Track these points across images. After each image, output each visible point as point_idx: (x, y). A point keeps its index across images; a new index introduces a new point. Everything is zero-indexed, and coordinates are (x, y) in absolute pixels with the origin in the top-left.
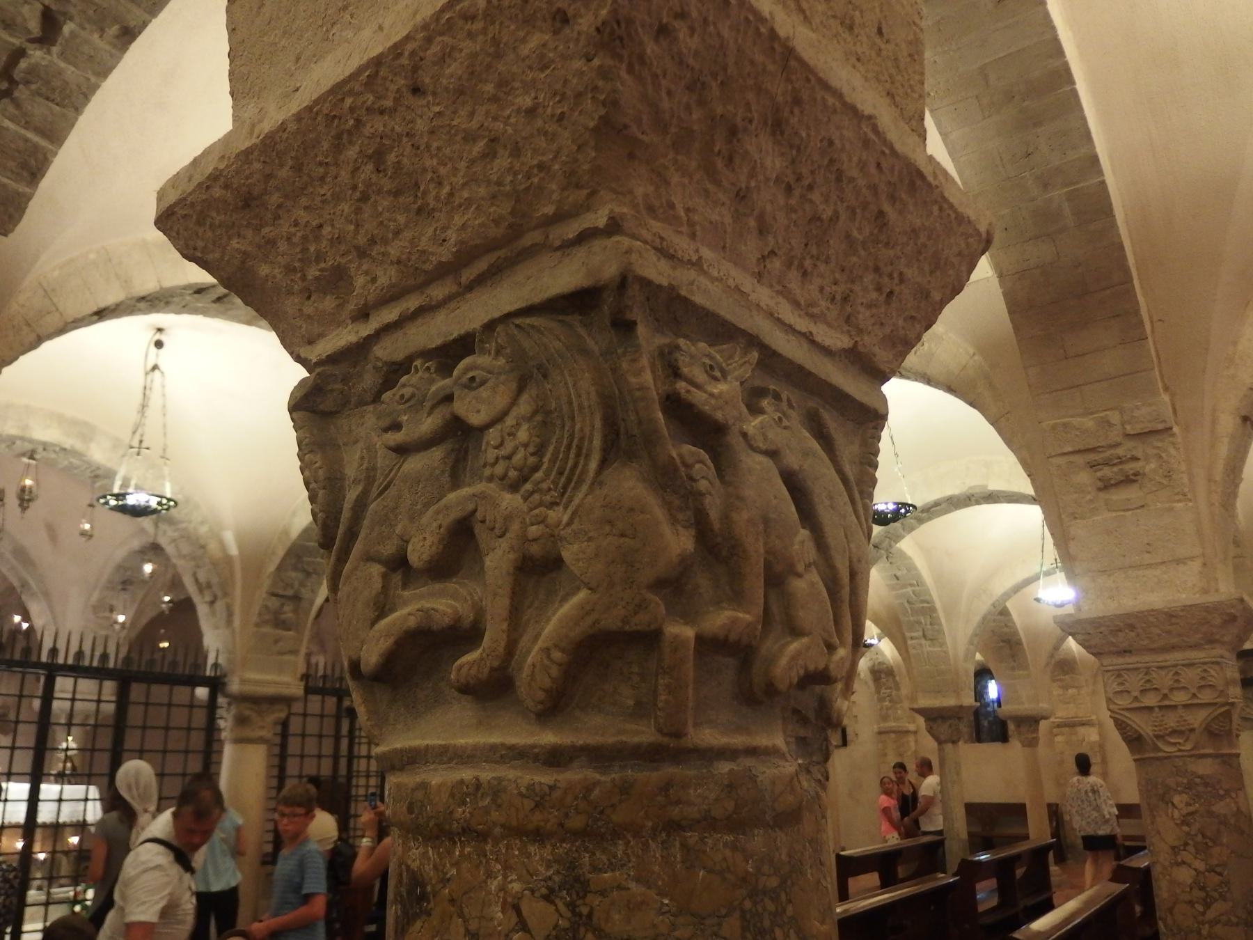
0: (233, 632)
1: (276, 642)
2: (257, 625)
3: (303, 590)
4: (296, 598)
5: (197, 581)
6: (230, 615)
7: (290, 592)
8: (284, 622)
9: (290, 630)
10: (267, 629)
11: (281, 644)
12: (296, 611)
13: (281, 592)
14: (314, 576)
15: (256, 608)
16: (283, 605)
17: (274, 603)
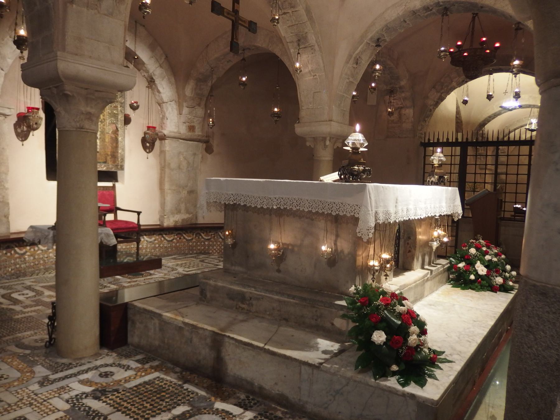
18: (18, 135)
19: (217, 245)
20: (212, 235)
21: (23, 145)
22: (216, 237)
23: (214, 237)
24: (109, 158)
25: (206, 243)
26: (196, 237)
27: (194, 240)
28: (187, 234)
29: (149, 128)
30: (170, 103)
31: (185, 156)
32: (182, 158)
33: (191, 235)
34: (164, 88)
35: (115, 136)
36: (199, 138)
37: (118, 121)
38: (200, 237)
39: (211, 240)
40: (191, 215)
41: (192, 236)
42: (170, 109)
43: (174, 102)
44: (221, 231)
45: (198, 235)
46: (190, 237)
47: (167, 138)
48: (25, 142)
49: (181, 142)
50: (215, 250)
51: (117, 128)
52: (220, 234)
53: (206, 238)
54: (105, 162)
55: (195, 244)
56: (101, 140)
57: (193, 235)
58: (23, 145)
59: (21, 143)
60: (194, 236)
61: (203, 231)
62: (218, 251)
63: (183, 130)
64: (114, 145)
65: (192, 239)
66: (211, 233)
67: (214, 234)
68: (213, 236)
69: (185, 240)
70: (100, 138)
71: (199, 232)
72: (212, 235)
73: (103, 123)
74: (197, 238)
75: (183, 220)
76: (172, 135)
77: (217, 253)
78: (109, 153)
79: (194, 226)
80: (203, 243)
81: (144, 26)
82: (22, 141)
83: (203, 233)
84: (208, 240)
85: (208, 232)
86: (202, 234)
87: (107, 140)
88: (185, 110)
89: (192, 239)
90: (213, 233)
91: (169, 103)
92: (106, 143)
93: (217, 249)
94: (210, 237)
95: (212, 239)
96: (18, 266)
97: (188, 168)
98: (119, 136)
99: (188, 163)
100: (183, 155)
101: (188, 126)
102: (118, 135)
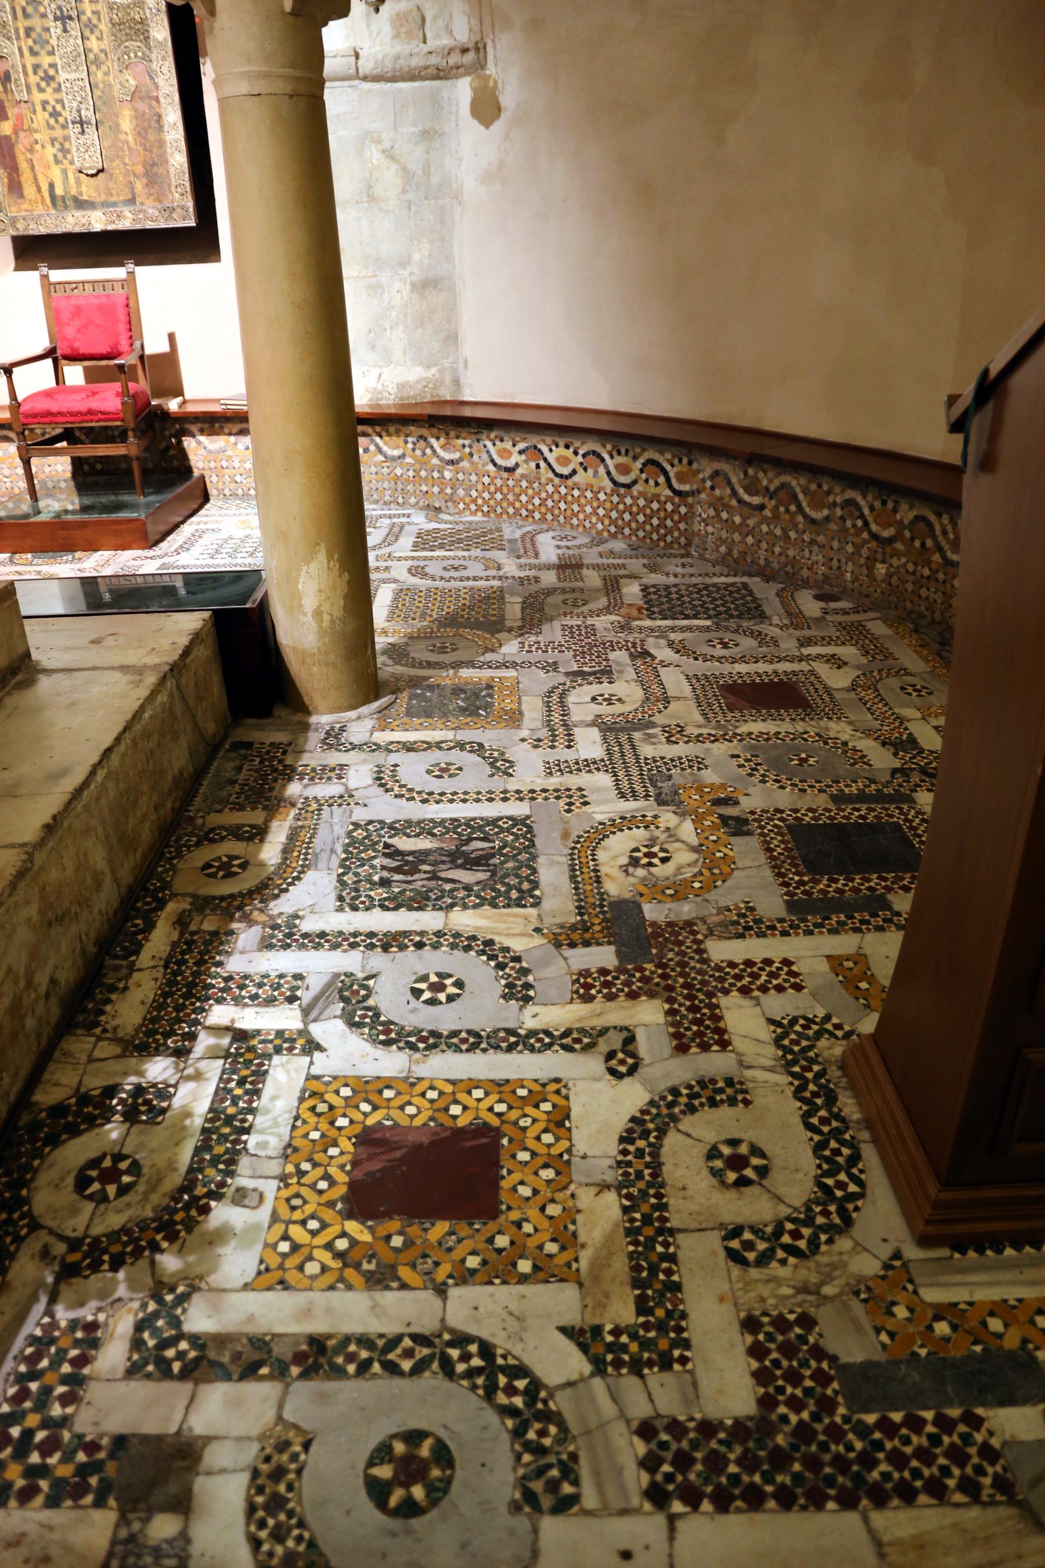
19: (480, 487)
20: (464, 446)
22: (476, 457)
23: (471, 455)
24: (139, 187)
25: (448, 475)
26: (414, 450)
27: (408, 460)
28: (387, 439)
31: (387, 145)
32: (374, 155)
33: (401, 440)
35: (151, 107)
36: (434, 60)
38: (428, 451)
39: (462, 464)
40: (434, 370)
41: (402, 444)
44: (493, 435)
45: (422, 443)
46: (397, 447)
49: (369, 91)
50: (474, 501)
52: (489, 444)
53: (448, 456)
54: (132, 201)
55: (411, 473)
57: (406, 442)
60: (410, 446)
61: (435, 431)
62: (485, 509)
65: (403, 456)
66: (460, 442)
67: (470, 446)
68: (467, 450)
69: (435, 461)
71: (425, 432)
72: (464, 446)
73: (104, 68)
74: (418, 452)
75: (402, 386)
77: (467, 513)
79: (448, 412)
80: (436, 475)
83: (438, 439)
84: (452, 462)
85: (452, 434)
86: (433, 441)
89: (403, 456)
90: (467, 442)
92: (122, 137)
93: (480, 501)
94: (456, 456)
95: (465, 464)
97: (404, 192)
98: (162, 100)
99: (406, 174)
100: (379, 142)
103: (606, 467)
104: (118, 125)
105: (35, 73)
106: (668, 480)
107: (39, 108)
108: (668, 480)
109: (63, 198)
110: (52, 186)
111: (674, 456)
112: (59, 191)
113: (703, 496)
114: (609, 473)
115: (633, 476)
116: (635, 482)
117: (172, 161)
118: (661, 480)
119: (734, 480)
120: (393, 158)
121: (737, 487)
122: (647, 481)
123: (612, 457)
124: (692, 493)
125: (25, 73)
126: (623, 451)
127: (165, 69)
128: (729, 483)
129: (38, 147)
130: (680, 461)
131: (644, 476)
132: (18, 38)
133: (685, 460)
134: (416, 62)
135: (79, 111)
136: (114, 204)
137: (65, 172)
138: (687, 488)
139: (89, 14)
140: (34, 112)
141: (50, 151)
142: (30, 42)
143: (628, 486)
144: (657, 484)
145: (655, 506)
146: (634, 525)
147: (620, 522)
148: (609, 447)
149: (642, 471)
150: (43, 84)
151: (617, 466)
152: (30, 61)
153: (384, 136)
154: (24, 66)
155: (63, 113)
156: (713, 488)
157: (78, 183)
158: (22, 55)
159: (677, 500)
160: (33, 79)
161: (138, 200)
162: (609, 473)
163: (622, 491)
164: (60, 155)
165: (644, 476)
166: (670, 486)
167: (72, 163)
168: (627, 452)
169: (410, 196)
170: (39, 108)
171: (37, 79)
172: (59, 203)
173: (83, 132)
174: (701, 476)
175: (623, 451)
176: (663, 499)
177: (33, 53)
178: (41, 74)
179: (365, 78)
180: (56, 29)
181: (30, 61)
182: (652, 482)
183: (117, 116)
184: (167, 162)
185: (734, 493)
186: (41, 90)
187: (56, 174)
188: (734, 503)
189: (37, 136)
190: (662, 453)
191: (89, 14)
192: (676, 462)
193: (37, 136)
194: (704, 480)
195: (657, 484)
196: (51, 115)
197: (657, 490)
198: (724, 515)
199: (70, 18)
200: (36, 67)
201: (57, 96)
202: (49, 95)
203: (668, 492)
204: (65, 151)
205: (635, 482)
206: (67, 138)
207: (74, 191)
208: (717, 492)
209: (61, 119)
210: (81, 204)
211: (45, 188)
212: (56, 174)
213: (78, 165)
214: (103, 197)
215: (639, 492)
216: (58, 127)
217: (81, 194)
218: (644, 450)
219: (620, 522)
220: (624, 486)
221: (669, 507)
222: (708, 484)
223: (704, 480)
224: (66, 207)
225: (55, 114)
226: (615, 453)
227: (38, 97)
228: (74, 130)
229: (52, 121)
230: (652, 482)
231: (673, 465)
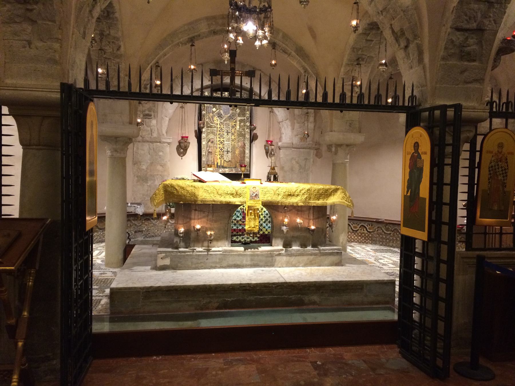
0: (424, 68)
1: (462, 72)
2: (443, 59)
3: (486, 22)
4: (480, 30)
5: (393, 32)
6: (420, 53)
7: (474, 25)
8: (469, 54)
9: (474, 61)
10: (453, 62)
11: (466, 74)
12: (480, 43)
13: (465, 26)
14: (496, 6)
15: (442, 44)
16: (467, 39)
17: (459, 37)
18: (179, 154)
21: (182, 159)
29: (267, 141)
30: (286, 121)
31: (297, 160)
32: (294, 162)
34: (279, 112)
35: (243, 150)
36: (309, 146)
37: (245, 139)
42: (285, 126)
43: (288, 120)
47: (281, 148)
48: (183, 157)
49: (294, 150)
51: (244, 144)
54: (235, 167)
56: (232, 153)
58: (182, 159)
59: (181, 158)
63: (296, 141)
64: (242, 155)
70: (231, 151)
73: (234, 142)
76: (285, 145)
78: (238, 161)
81: (260, 70)
82: (182, 156)
87: (237, 152)
88: (297, 126)
91: (284, 121)
96: (170, 230)
97: (300, 170)
98: (246, 149)
99: (300, 166)
100: (295, 160)
101: (300, 138)
102: (245, 148)
103: (351, 227)
104: (235, 152)
105: (219, 141)
106: (366, 229)
107: (218, 148)
108: (366, 229)
109: (220, 166)
110: (217, 163)
111: (368, 224)
112: (219, 164)
113: (375, 232)
114: (351, 228)
115: (358, 229)
116: (358, 230)
117: (246, 160)
118: (365, 229)
119: (383, 229)
120: (298, 163)
121: (384, 230)
122: (361, 230)
123: (352, 225)
124: (373, 232)
125: (217, 141)
126: (355, 223)
127: (248, 143)
128: (382, 229)
129: (216, 155)
130: (369, 225)
131: (360, 229)
132: (217, 135)
133: (371, 225)
134: (305, 146)
135: (227, 149)
136: (231, 168)
137: (221, 161)
138: (371, 231)
139: (233, 132)
140: (217, 149)
141: (219, 156)
142: (219, 136)
143: (356, 231)
144: (364, 230)
145: (363, 235)
146: (358, 239)
147: (354, 239)
148: (352, 223)
149: (360, 228)
150: (220, 144)
151: (353, 227)
152: (218, 139)
153: (296, 159)
154: (217, 140)
155: (224, 149)
156: (378, 230)
157: (224, 163)
158: (217, 138)
159: (369, 233)
160: (218, 143)
161: (237, 167)
162: (351, 228)
163: (355, 232)
164: (221, 157)
165: (360, 229)
166: (367, 231)
167: (224, 159)
168: (356, 224)
169: (301, 170)
170: (218, 148)
171: (219, 143)
172: (218, 167)
173: (227, 153)
174: (375, 228)
175: (355, 223)
176: (365, 233)
177: (219, 138)
178: (220, 142)
179: (294, 148)
180: (226, 134)
181: (218, 139)
182: (362, 230)
183: (235, 151)
184: (245, 160)
185: (383, 231)
186: (219, 145)
187: (219, 161)
188: (383, 233)
189: (216, 153)
190: (365, 224)
191: (233, 132)
192: (368, 225)
193: (216, 153)
194: (375, 229)
195: (364, 230)
196: (220, 150)
197: (364, 232)
198: (381, 236)
199: (229, 132)
200: (219, 141)
201: (223, 146)
202: (221, 146)
203: (367, 232)
204: (222, 157)
205: (358, 230)
206: (223, 154)
207: (222, 165)
208: (379, 231)
209: (223, 151)
210: (223, 167)
211: (216, 163)
212: (219, 161)
213: (225, 160)
214: (229, 166)
215: (359, 232)
216: (222, 152)
217: (224, 165)
218: (360, 223)
219: (354, 239)
220: (355, 231)
221: (367, 235)
222: (377, 230)
223: (375, 229)
224: (220, 168)
225: (221, 149)
226: (353, 224)
227: (218, 146)
228: (225, 153)
229: (221, 151)
230: (362, 230)
231: (368, 226)
